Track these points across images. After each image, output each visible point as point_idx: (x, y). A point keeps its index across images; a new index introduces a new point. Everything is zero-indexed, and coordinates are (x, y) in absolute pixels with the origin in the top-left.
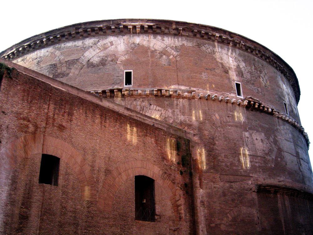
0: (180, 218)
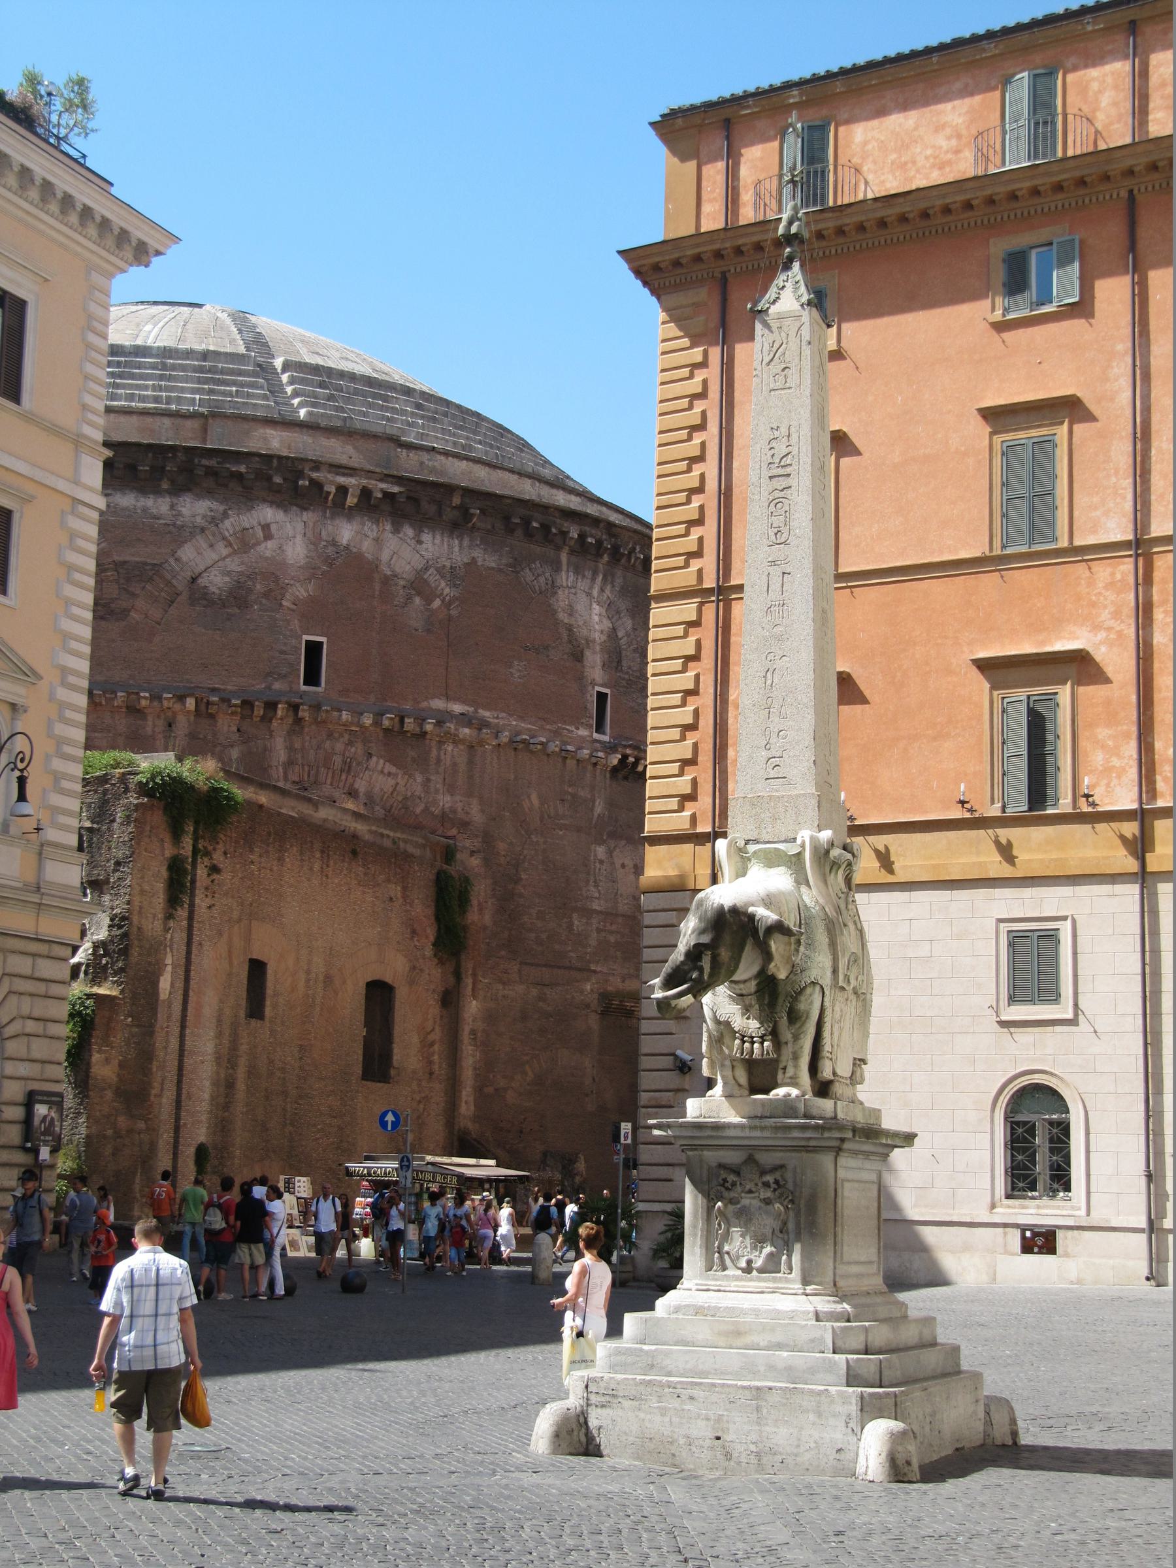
0: (431, 1074)
